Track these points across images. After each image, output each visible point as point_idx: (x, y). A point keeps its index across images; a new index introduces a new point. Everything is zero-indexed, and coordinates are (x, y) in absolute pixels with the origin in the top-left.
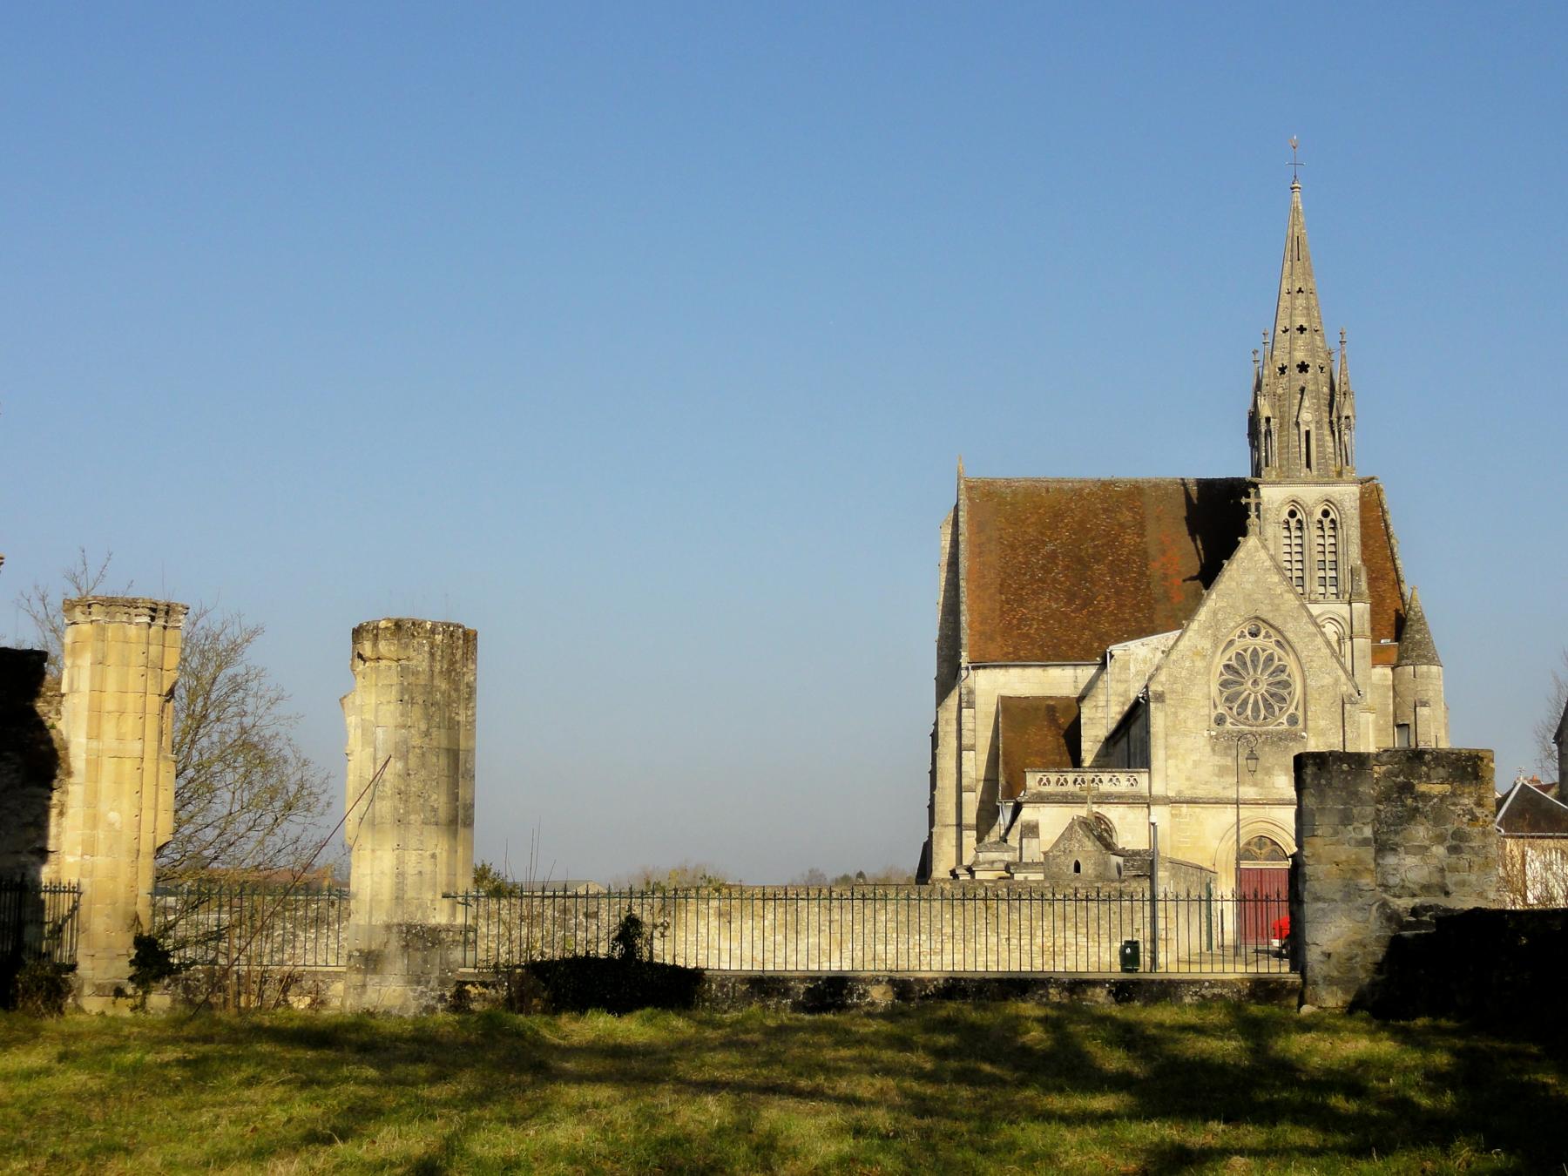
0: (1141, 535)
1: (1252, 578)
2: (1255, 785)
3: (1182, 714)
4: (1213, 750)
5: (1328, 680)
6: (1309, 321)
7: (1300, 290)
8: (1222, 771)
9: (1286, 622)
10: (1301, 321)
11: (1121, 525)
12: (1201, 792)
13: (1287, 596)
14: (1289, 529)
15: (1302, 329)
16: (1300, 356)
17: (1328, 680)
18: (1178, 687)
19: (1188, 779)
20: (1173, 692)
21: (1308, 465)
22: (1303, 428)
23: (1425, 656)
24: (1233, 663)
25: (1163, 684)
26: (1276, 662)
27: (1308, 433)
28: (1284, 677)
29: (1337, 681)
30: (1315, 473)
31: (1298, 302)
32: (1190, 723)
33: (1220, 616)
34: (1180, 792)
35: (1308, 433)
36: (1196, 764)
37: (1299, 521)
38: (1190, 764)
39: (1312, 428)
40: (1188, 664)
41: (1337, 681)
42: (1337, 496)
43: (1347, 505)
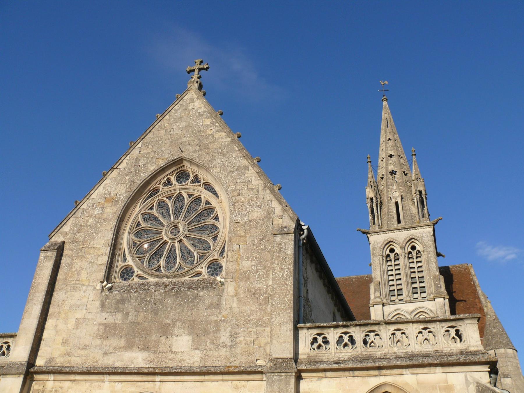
1: (183, 124)
2: (146, 348)
3: (77, 265)
4: (103, 306)
5: (257, 214)
7: (389, 139)
8: (108, 331)
9: (213, 158)
10: (391, 152)
12: (77, 361)
13: (217, 135)
15: (391, 156)
16: (391, 168)
17: (257, 214)
18: (81, 237)
19: (65, 342)
20: (74, 241)
21: (399, 222)
24: (154, 212)
25: (66, 234)
26: (203, 205)
27: (397, 203)
28: (210, 221)
29: (269, 214)
30: (402, 224)
31: (388, 145)
32: (83, 276)
33: (141, 162)
34: (51, 360)
35: (397, 203)
36: (78, 323)
38: (72, 322)
39: (399, 200)
40: (96, 212)
41: (269, 214)
42: (418, 235)
43: (425, 239)
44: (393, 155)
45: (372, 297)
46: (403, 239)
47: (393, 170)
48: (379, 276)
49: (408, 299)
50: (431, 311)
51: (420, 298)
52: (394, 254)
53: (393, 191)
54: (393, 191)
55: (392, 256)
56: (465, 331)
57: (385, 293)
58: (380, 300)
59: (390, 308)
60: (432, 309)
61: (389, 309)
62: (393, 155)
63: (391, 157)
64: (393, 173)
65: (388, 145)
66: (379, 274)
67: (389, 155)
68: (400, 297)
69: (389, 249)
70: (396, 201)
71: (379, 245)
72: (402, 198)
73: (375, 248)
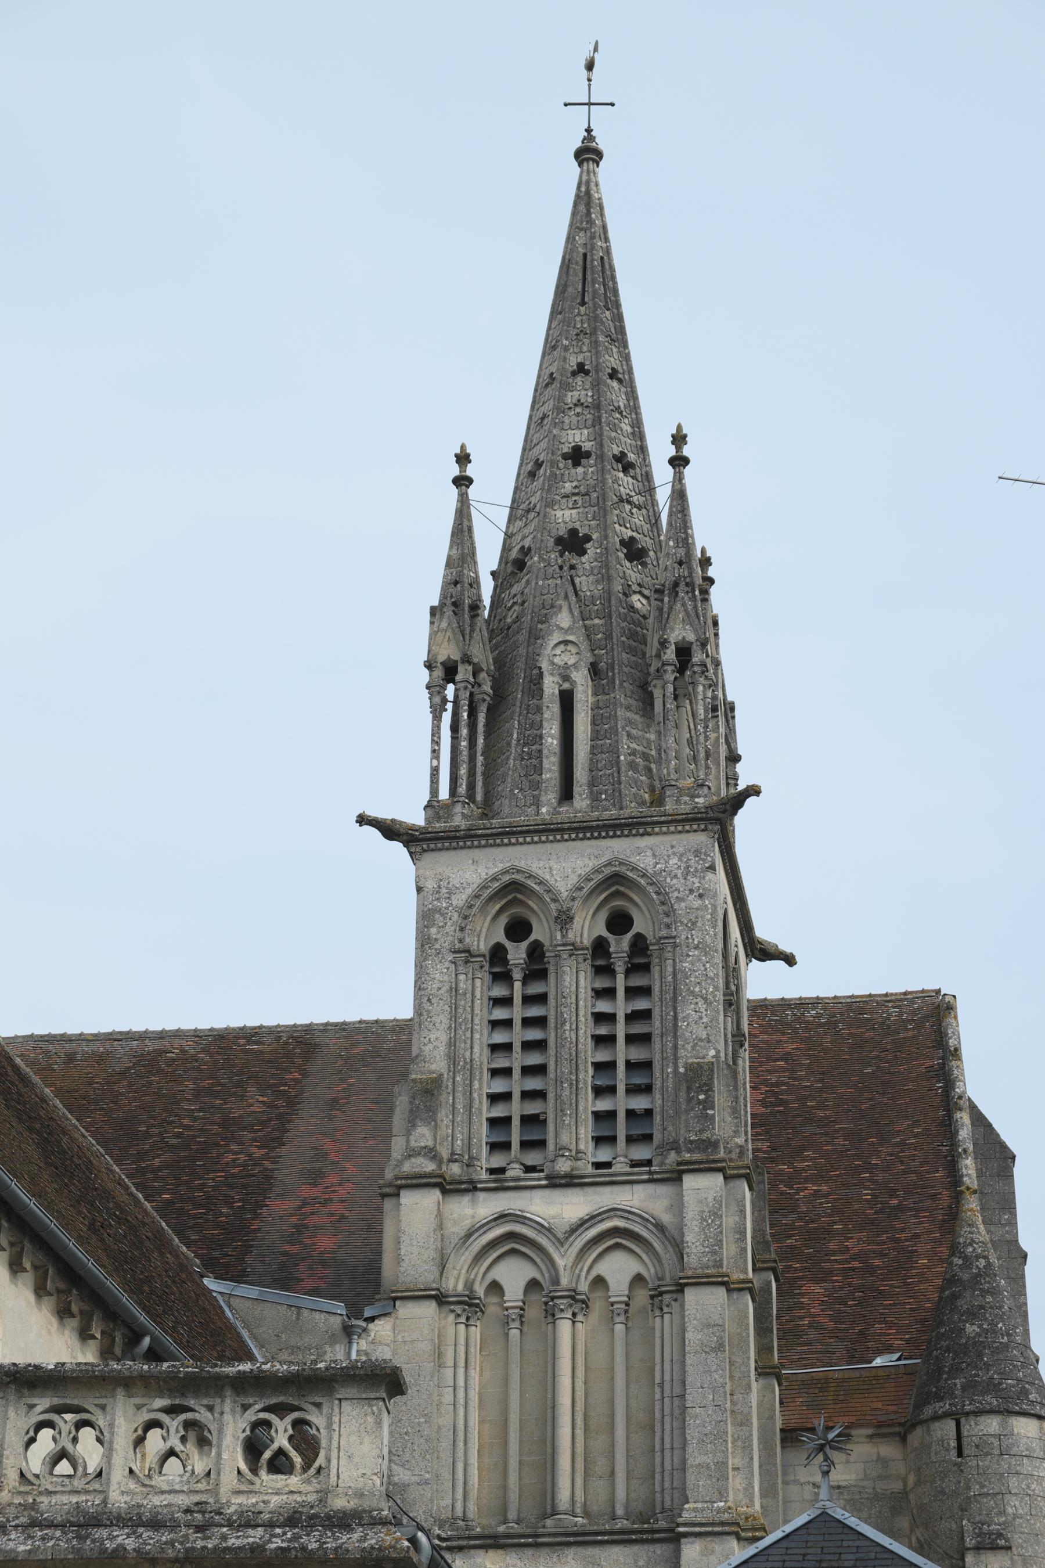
0: (274, 1141)
6: (598, 438)
7: (581, 369)
10: (578, 437)
11: (226, 1122)
14: (503, 977)
15: (577, 456)
22: (551, 686)
23: (992, 1387)
27: (567, 700)
30: (581, 802)
31: (571, 398)
35: (567, 700)
37: (536, 952)
39: (581, 679)
42: (645, 862)
44: (588, 455)
45: (398, 1146)
46: (574, 880)
47: (573, 532)
48: (442, 1049)
49: (563, 1166)
50: (660, 1227)
51: (620, 1167)
52: (524, 945)
53: (556, 637)
54: (556, 637)
55: (517, 954)
56: (329, 1426)
57: (460, 1128)
58: (430, 1167)
59: (474, 1202)
60: (666, 1219)
61: (469, 1211)
62: (588, 455)
63: (576, 464)
64: (573, 543)
65: (571, 398)
66: (444, 1038)
67: (566, 449)
68: (533, 1158)
69: (503, 921)
70: (566, 686)
71: (460, 899)
72: (595, 670)
73: (439, 911)
